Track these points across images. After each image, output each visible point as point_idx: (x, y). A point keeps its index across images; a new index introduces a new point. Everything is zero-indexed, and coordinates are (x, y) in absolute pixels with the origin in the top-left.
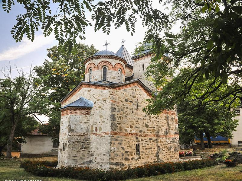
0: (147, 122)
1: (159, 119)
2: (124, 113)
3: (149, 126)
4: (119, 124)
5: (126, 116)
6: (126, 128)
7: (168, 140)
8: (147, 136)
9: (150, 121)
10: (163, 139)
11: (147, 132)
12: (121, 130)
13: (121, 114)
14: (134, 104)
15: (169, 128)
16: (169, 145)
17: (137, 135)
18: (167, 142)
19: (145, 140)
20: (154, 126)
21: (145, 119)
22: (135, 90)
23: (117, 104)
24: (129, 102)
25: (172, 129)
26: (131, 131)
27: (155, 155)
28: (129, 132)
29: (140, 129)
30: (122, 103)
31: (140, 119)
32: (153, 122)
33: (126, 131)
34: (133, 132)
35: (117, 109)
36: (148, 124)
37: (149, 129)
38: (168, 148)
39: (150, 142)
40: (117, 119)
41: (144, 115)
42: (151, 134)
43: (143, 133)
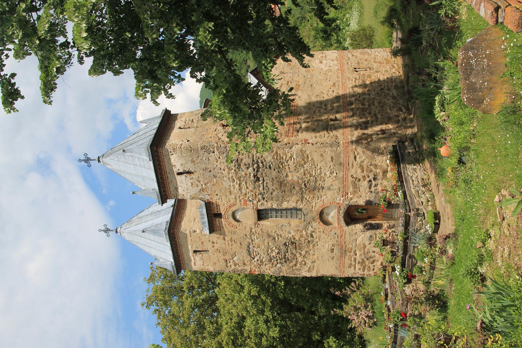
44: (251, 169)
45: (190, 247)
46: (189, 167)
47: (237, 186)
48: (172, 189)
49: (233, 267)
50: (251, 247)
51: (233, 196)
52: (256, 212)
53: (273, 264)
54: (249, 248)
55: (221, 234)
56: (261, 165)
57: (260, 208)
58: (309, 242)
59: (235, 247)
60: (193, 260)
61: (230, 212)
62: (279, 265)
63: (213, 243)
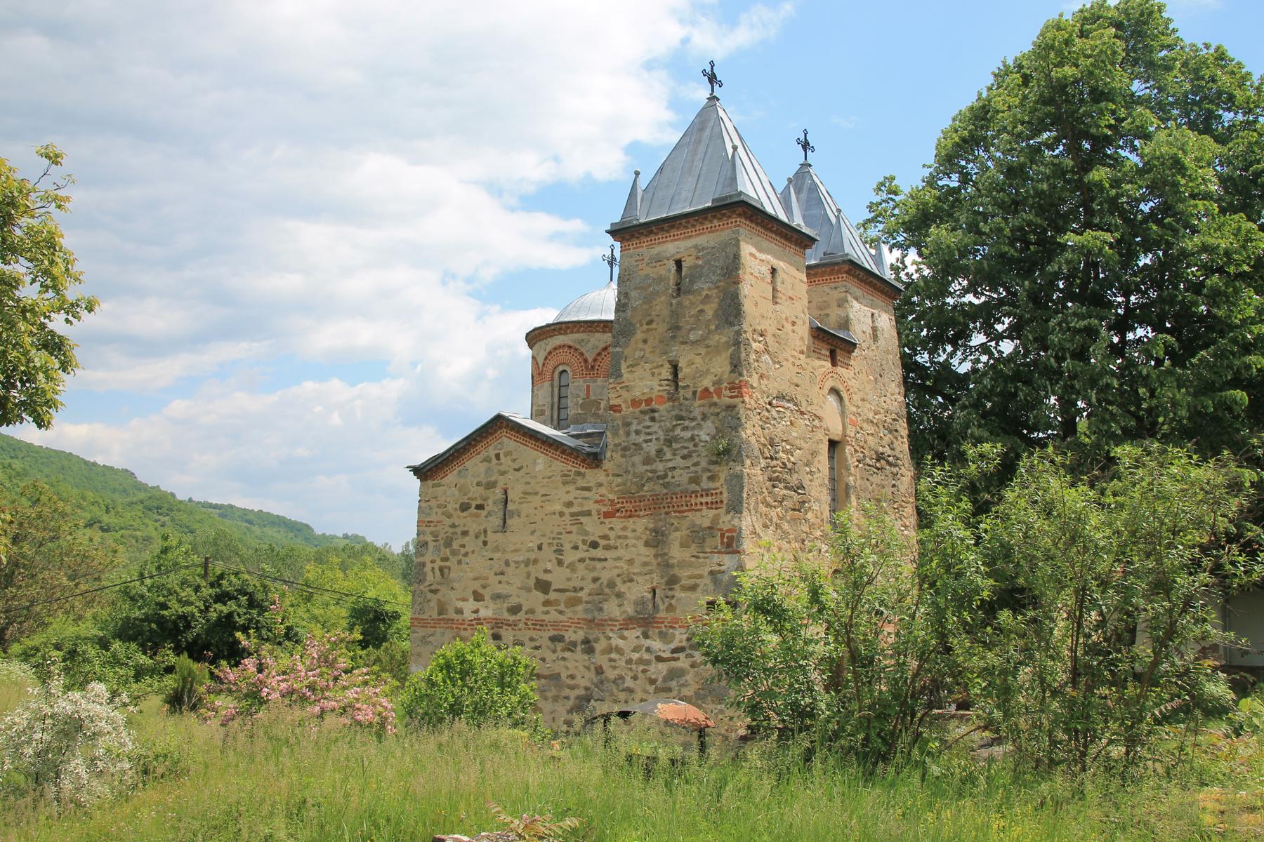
0: (546, 571)
1: (607, 548)
2: (454, 553)
3: (553, 587)
4: (435, 592)
5: (460, 562)
6: (460, 604)
7: (656, 644)
8: (540, 625)
9: (560, 563)
10: (623, 638)
11: (545, 609)
12: (442, 610)
13: (446, 559)
14: (489, 514)
15: (672, 581)
16: (663, 667)
17: (497, 624)
18: (648, 649)
19: (534, 644)
20: (578, 584)
21: (535, 561)
22: (494, 461)
23: (432, 529)
24: (473, 510)
25: (693, 588)
26: (476, 611)
27: (570, 704)
28: (468, 615)
29: (514, 601)
30: (448, 522)
31: (512, 564)
32: (572, 567)
33: (459, 611)
34: (483, 613)
35: (431, 545)
36: (547, 577)
37: (553, 596)
38: (652, 682)
39: (554, 651)
40: (430, 577)
41: (531, 544)
42: (561, 618)
43: (521, 615)
44: (890, 452)
45: (782, 264)
46: (881, 342)
47: (871, 416)
48: (858, 292)
49: (755, 345)
50: (791, 405)
51: (860, 403)
52: (836, 438)
53: (764, 445)
54: (788, 401)
55: (808, 348)
56: (894, 470)
57: (848, 450)
58: (803, 541)
59: (788, 371)
60: (758, 254)
61: (841, 387)
62: (763, 463)
63: (794, 324)
